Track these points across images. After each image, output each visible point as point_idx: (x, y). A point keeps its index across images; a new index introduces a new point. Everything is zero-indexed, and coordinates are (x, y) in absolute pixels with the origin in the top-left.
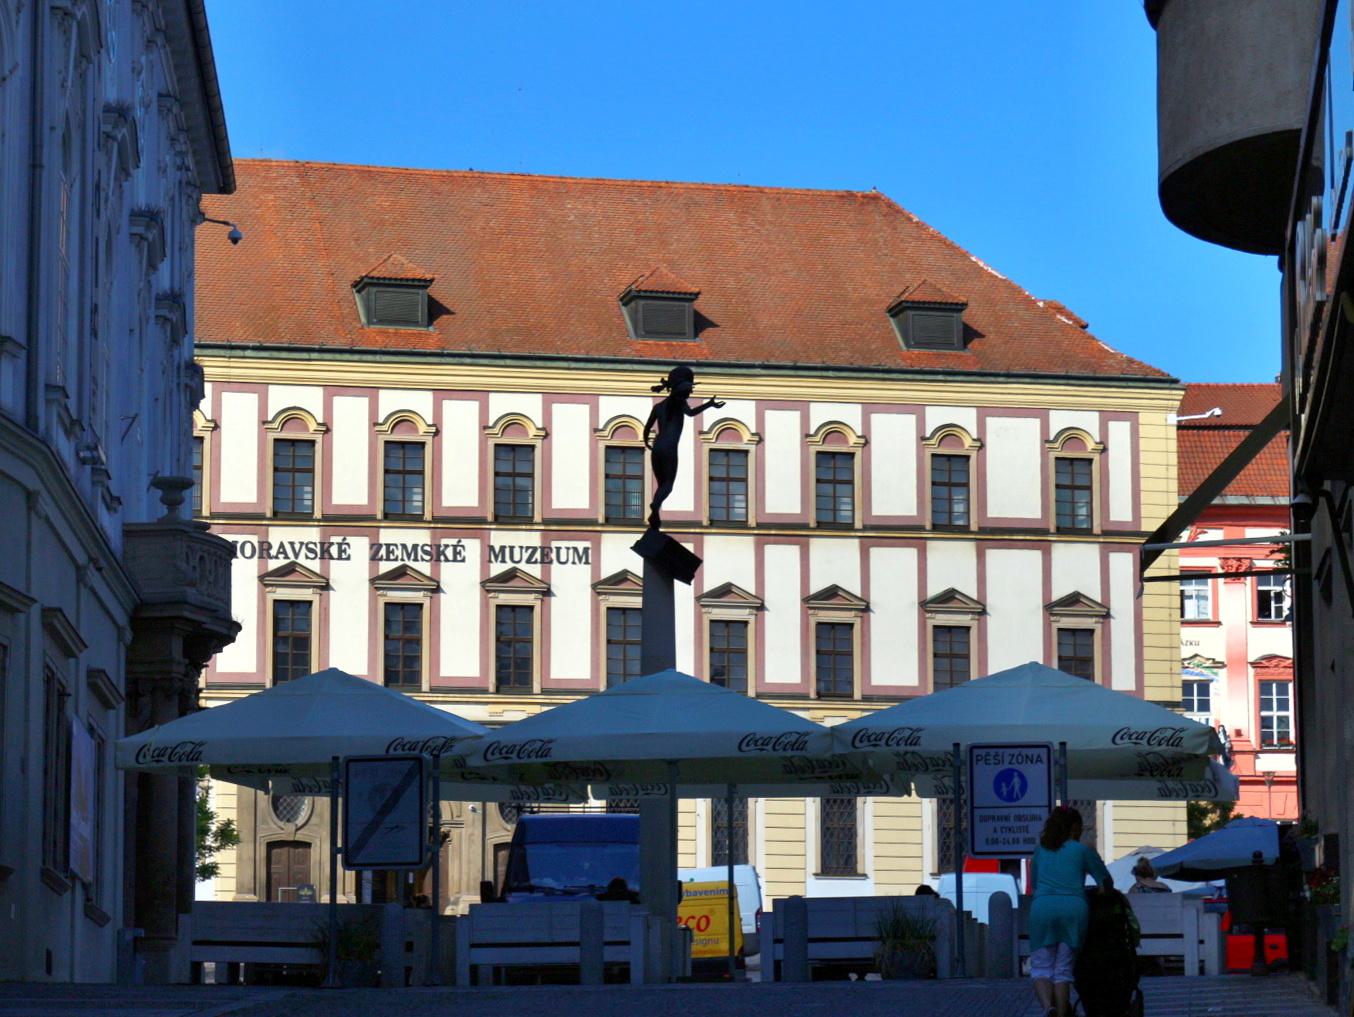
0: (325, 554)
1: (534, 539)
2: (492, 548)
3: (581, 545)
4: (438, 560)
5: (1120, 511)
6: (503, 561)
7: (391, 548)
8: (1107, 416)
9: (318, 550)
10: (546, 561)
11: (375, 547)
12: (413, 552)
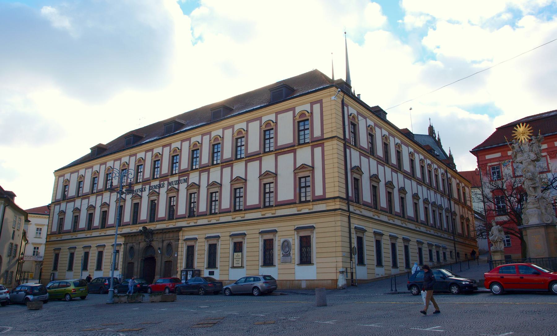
0: (142, 191)
1: (176, 178)
2: (169, 182)
3: (185, 178)
4: (160, 188)
5: (317, 133)
6: (171, 185)
8: (312, 104)
10: (179, 184)
11: (150, 187)
12: (155, 187)
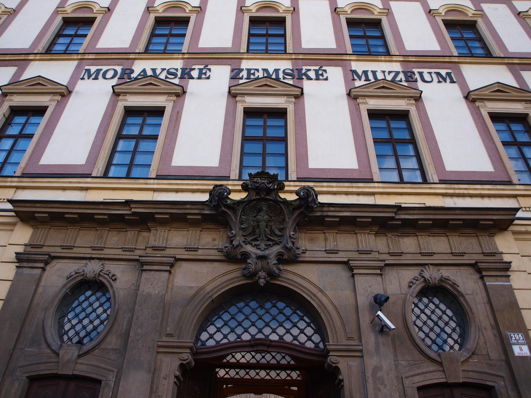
2: (354, 72)
3: (443, 72)
7: (252, 72)
9: (179, 73)
